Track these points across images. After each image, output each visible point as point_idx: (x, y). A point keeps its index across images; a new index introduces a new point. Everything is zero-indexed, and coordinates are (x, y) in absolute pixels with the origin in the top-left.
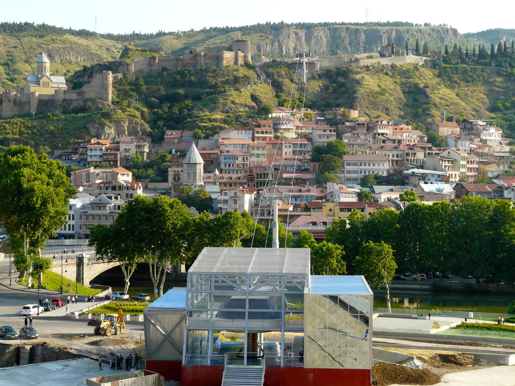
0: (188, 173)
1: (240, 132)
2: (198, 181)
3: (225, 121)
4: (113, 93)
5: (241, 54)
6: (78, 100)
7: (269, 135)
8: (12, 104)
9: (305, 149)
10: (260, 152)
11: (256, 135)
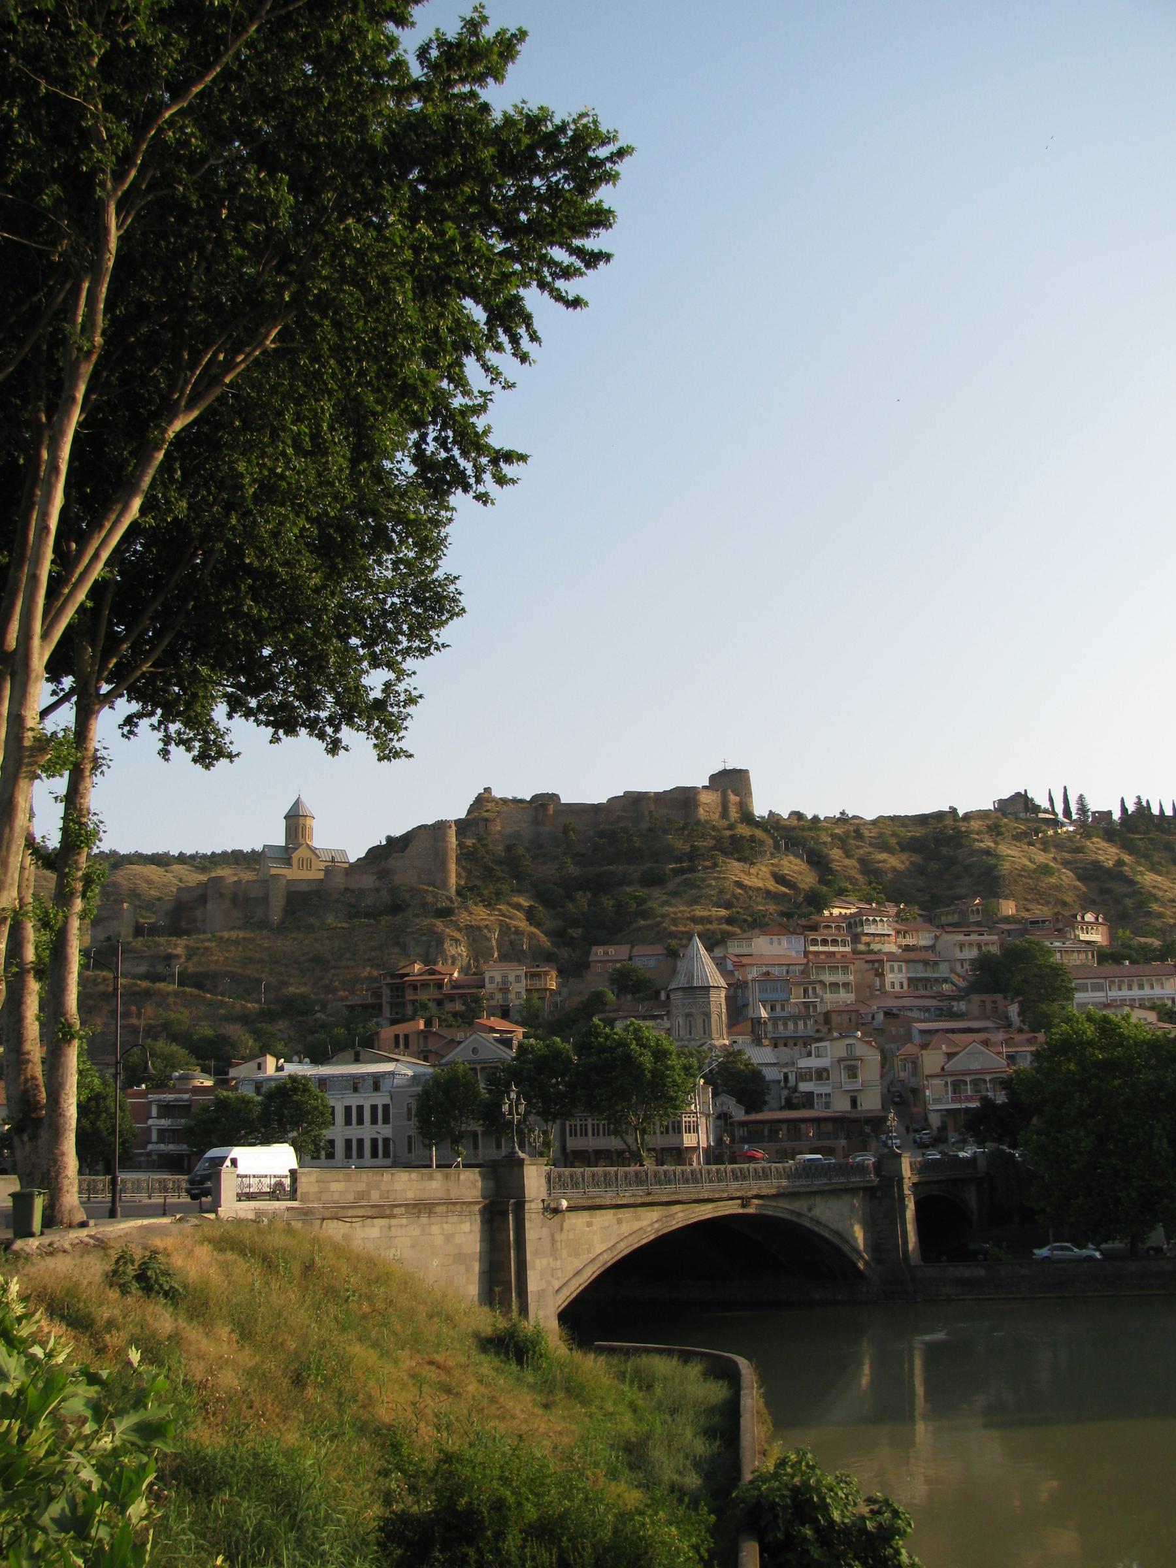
0: (689, 1015)
1: (775, 938)
2: (714, 1035)
3: (730, 921)
4: (458, 876)
5: (733, 798)
6: (378, 890)
7: (842, 949)
9: (936, 975)
10: (839, 978)
11: (812, 949)
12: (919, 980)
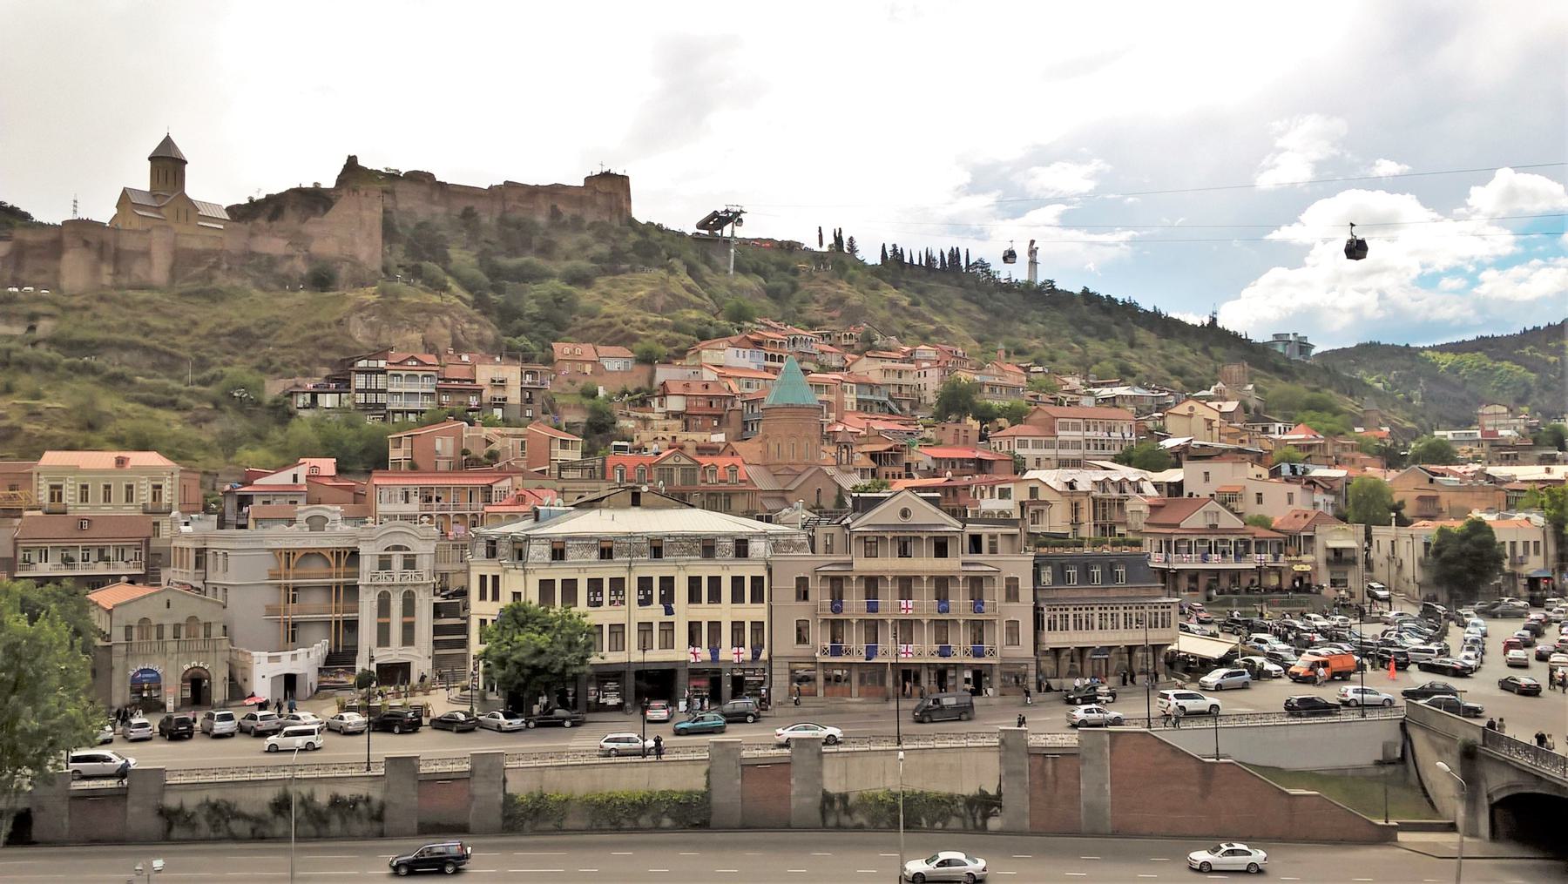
8: (93, 256)
12: (864, 401)
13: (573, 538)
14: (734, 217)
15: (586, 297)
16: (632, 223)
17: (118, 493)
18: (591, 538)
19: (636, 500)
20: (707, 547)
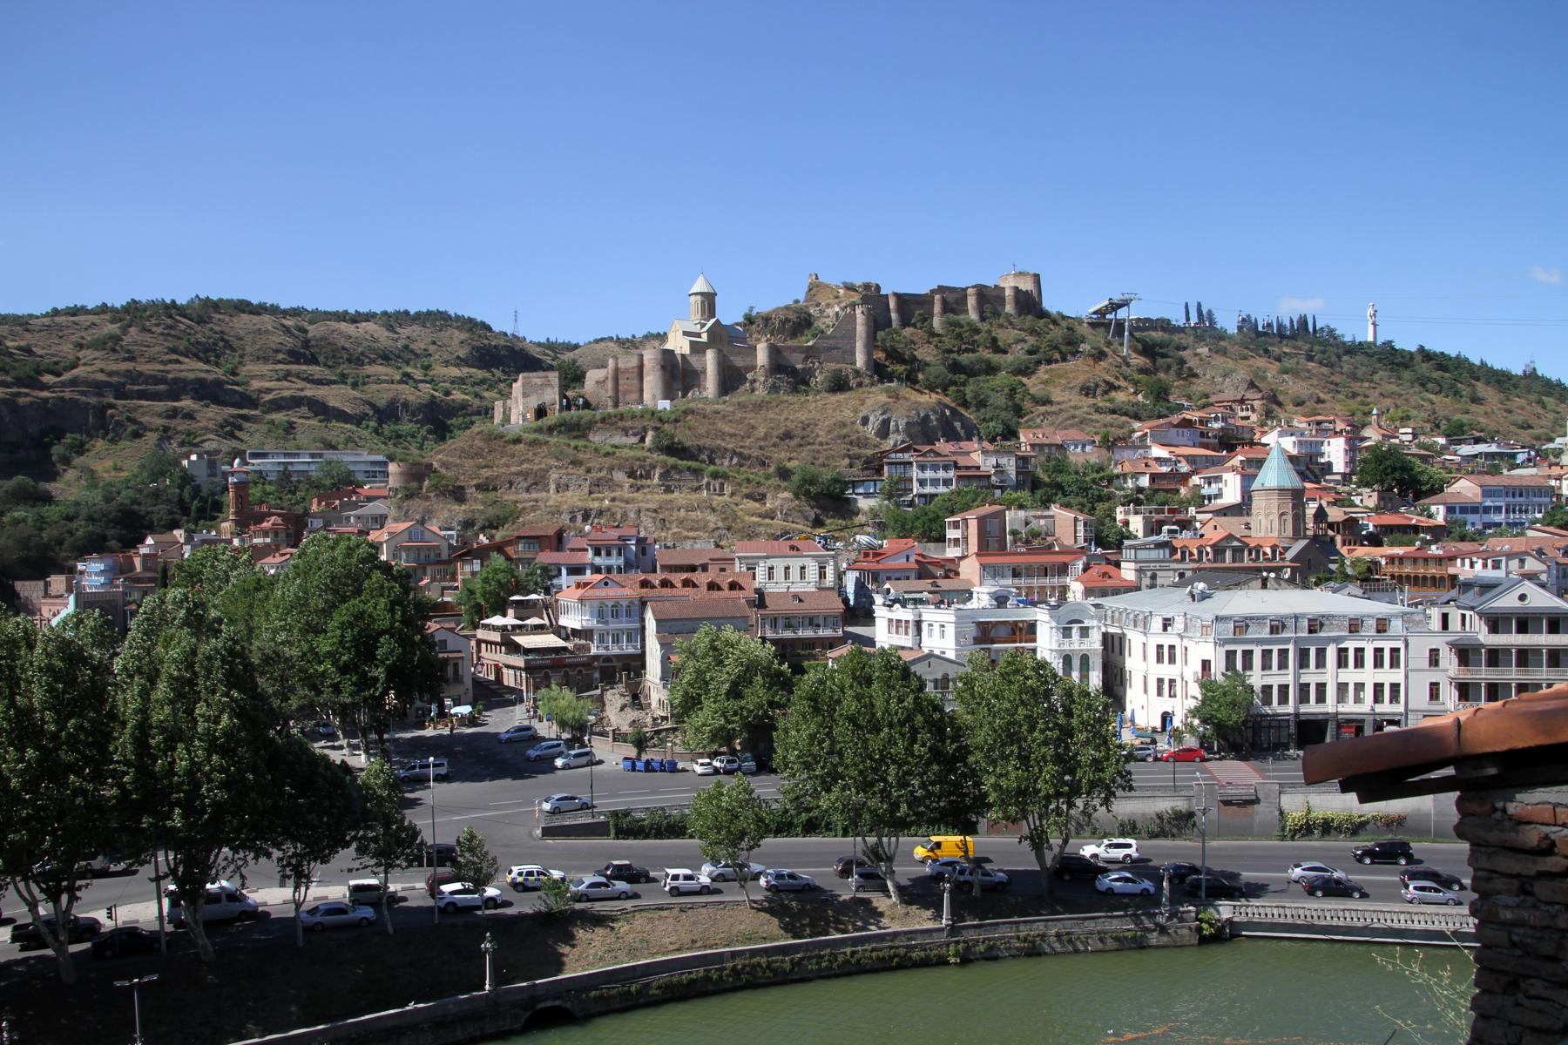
13: (1251, 618)
14: (1124, 304)
15: (1033, 384)
16: (1043, 314)
17: (795, 574)
18: (1264, 618)
19: (1264, 586)
20: (1355, 626)
